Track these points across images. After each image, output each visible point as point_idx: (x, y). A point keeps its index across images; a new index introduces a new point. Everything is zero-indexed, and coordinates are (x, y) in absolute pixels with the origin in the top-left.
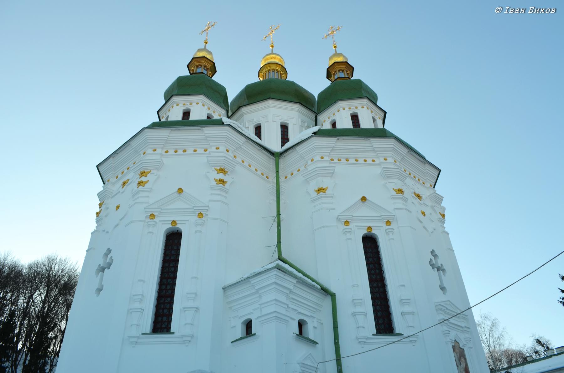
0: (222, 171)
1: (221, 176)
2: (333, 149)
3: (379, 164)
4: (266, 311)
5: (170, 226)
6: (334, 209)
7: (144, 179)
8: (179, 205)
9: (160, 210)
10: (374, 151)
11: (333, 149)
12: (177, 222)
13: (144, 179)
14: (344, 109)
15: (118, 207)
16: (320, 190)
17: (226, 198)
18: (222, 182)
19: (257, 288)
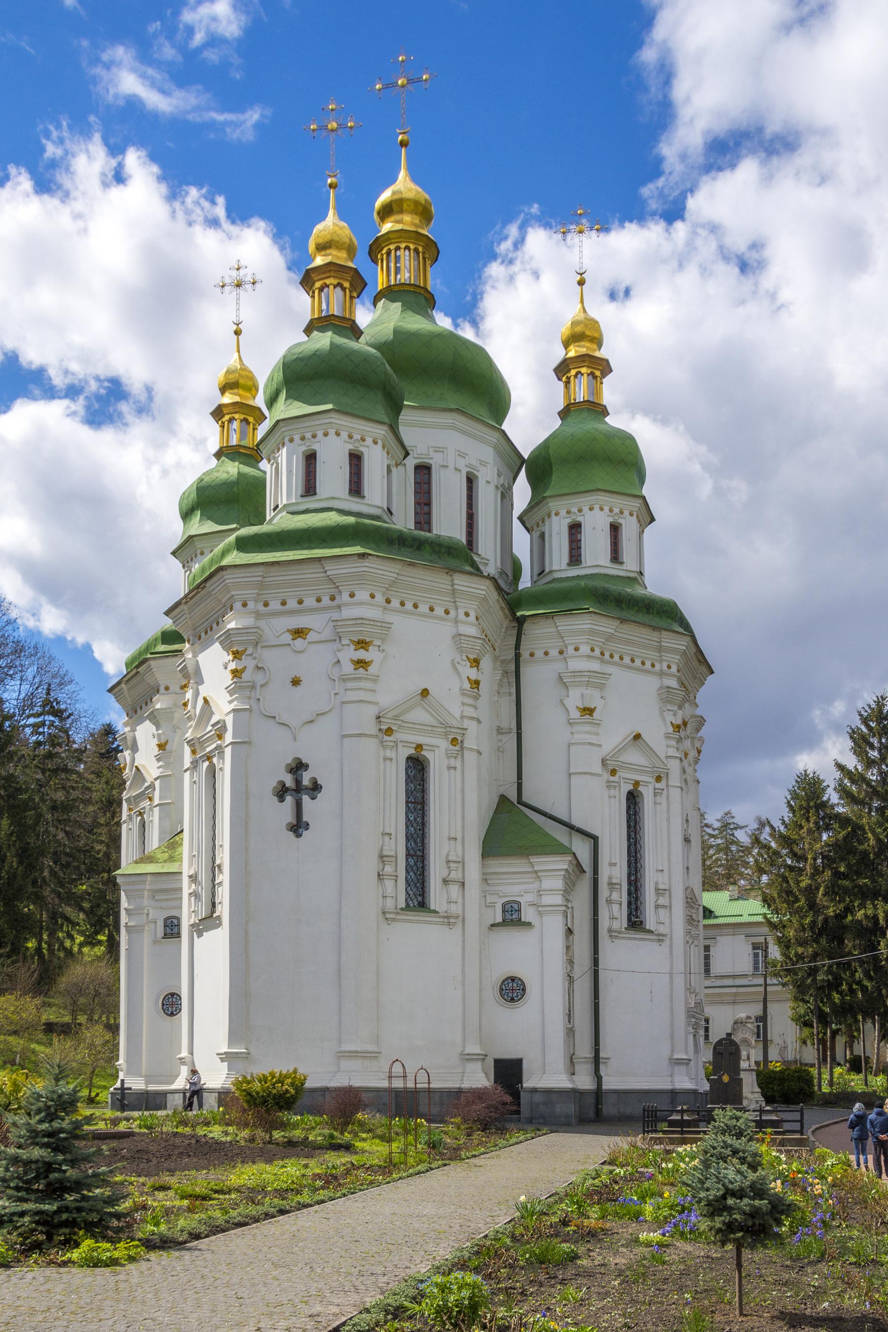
0: (476, 663)
1: (473, 674)
2: (610, 638)
3: (661, 674)
4: (547, 900)
5: (413, 751)
6: (600, 746)
7: (362, 654)
8: (419, 715)
9: (400, 723)
10: (660, 649)
11: (610, 638)
12: (425, 747)
13: (362, 654)
14: (602, 509)
15: (296, 682)
16: (588, 711)
17: (476, 708)
18: (477, 683)
19: (536, 868)
